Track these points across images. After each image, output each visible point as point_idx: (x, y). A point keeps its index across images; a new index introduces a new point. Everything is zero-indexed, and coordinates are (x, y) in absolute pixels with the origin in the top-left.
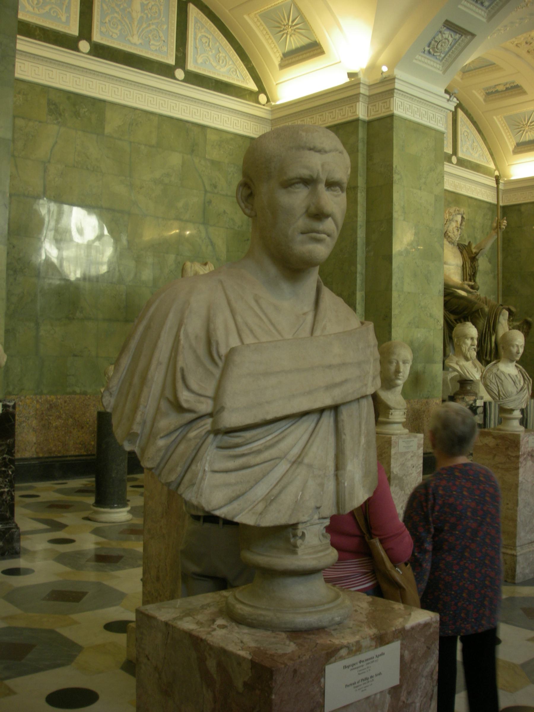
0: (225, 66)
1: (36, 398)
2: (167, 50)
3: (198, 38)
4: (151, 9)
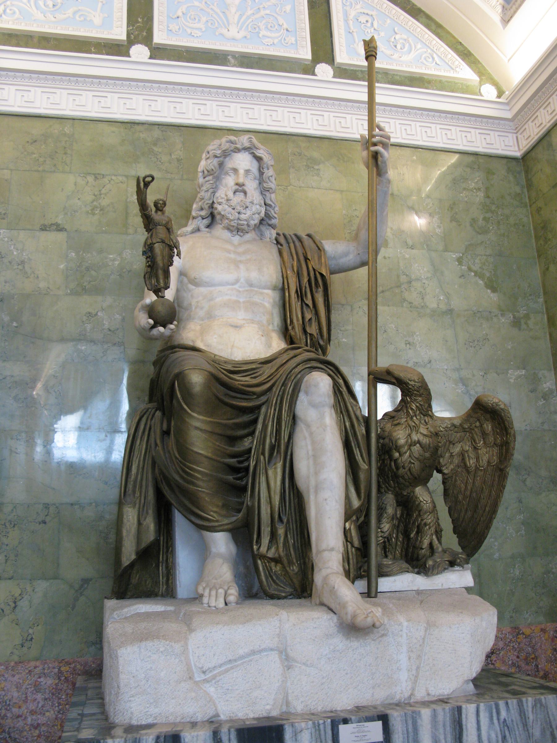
1: (11, 712)
2: (296, 41)
3: (351, 17)
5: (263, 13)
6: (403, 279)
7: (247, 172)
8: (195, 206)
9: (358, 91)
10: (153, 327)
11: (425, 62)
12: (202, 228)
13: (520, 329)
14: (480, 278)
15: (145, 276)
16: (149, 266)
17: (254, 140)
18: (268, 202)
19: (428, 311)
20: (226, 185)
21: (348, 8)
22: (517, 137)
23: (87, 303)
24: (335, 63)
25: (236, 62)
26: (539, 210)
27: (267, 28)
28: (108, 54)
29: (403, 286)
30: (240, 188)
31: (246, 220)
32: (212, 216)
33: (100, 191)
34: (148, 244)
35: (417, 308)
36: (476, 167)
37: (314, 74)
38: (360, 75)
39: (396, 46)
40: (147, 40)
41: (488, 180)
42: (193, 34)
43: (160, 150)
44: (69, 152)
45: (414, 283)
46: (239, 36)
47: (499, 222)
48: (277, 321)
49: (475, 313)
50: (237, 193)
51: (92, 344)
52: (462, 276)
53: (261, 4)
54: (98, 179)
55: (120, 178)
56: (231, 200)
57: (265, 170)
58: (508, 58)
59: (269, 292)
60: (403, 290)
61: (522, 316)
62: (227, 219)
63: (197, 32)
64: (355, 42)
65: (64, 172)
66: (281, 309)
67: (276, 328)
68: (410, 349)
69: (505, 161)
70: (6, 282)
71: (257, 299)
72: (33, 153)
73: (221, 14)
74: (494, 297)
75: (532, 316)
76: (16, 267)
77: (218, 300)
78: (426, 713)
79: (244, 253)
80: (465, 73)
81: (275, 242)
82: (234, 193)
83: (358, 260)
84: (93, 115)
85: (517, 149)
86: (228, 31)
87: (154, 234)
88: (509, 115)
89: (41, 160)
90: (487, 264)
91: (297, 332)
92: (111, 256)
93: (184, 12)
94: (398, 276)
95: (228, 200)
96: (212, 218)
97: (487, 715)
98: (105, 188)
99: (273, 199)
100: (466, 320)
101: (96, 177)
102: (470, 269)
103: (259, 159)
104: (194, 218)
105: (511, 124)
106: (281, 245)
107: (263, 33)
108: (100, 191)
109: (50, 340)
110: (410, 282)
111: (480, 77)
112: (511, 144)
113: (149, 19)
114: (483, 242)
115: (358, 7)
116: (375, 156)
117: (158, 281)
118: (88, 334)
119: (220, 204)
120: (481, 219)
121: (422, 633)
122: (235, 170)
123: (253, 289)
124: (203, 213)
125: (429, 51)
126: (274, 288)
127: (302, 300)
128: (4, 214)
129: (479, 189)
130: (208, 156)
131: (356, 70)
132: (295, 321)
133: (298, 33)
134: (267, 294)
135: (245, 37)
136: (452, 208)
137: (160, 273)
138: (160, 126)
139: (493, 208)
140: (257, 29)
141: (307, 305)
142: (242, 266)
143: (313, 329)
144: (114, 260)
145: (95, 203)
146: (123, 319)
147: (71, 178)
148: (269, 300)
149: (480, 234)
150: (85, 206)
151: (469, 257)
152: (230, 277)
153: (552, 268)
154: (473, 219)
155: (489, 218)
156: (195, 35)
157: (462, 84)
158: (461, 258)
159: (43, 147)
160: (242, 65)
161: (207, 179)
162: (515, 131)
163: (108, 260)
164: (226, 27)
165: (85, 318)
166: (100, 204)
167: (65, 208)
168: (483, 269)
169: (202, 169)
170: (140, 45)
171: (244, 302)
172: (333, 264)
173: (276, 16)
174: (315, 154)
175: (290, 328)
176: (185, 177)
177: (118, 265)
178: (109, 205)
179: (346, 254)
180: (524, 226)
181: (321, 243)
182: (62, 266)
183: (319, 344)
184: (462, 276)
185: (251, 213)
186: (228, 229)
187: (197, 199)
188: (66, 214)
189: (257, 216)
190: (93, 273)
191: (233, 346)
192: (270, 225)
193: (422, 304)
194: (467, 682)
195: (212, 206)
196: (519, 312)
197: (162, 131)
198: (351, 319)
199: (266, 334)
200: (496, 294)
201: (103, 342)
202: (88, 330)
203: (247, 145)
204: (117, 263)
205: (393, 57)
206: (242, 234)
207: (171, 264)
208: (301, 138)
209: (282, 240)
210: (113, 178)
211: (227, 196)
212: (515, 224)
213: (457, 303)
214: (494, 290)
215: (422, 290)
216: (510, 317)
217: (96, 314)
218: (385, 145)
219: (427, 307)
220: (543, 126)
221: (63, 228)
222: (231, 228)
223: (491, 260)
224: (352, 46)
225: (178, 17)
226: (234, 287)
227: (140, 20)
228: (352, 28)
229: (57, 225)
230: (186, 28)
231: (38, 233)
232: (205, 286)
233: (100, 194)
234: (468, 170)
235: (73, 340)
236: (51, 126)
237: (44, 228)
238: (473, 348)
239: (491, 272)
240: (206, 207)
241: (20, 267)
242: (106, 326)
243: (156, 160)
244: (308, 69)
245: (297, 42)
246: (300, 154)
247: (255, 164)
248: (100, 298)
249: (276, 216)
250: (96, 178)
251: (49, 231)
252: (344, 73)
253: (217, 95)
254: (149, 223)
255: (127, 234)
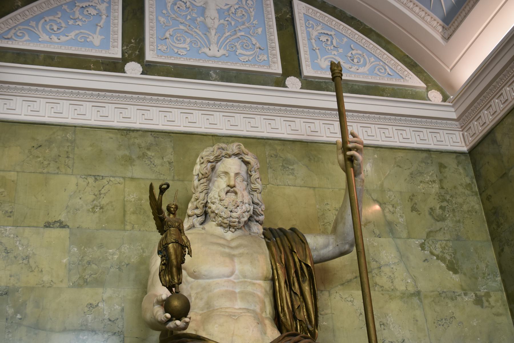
0: (365, 65)
2: (268, 57)
3: (313, 37)
4: (235, 14)
5: (239, 34)
7: (237, 174)
8: (190, 205)
9: (328, 100)
10: (170, 320)
11: (378, 73)
12: (197, 225)
13: (482, 307)
14: (441, 261)
15: (160, 273)
16: (164, 264)
17: (242, 147)
18: (256, 201)
19: (398, 294)
20: (219, 187)
21: (310, 30)
22: (463, 135)
23: (88, 295)
24: (302, 77)
25: (217, 77)
26: (489, 198)
27: (242, 46)
28: (105, 70)
29: (373, 272)
30: (231, 189)
31: (238, 218)
32: (206, 213)
33: (100, 191)
34: (164, 244)
35: (388, 291)
36: (429, 161)
37: (285, 86)
38: (324, 86)
39: (353, 60)
40: (140, 58)
41: (441, 172)
42: (179, 53)
43: (153, 154)
44: (71, 156)
45: (382, 268)
46: (218, 54)
47: (454, 210)
48: (269, 309)
49: (440, 294)
50: (229, 194)
51: (94, 333)
52: (426, 260)
53: (237, 27)
54: (98, 180)
55: (118, 179)
56: (223, 200)
57: (253, 173)
58: (451, 67)
59: (261, 282)
60: (374, 275)
61: (483, 294)
62: (221, 217)
63: (183, 51)
64: (318, 58)
65: (66, 174)
66: (272, 298)
67: (268, 316)
68: (384, 329)
69: (454, 156)
70: (11, 276)
71: (250, 289)
72: (38, 157)
73: (203, 36)
74: (456, 278)
75: (492, 294)
76: (21, 262)
77: (216, 291)
79: (237, 247)
80: (414, 81)
81: (263, 237)
82: (226, 193)
83: (337, 251)
84: (93, 123)
85: (464, 144)
86: (210, 50)
87: (168, 235)
88: (454, 116)
89: (46, 163)
90: (447, 248)
91: (287, 318)
92: (111, 251)
93: (171, 34)
95: (221, 200)
96: (206, 215)
98: (104, 189)
99: (260, 199)
100: (433, 301)
101: (96, 179)
102: (432, 253)
103: (247, 163)
104: (189, 216)
105: (457, 123)
106: (269, 239)
107: (239, 51)
108: (100, 191)
109: (52, 330)
110: (380, 268)
111: (426, 84)
112: (459, 140)
113: (141, 40)
114: (441, 228)
115: (319, 28)
116: (351, 159)
117: (173, 277)
118: (89, 324)
119: (213, 203)
120: (438, 208)
122: (226, 173)
123: (246, 280)
124: (198, 212)
125: (381, 63)
126: (266, 279)
127: (291, 289)
128: (11, 212)
129: (434, 181)
130: (202, 161)
131: (320, 82)
132: (286, 309)
133: (269, 51)
134: (259, 285)
135: (224, 55)
136: (412, 200)
137: (174, 270)
138: (153, 133)
139: (448, 197)
140: (234, 48)
141: (295, 293)
142: (236, 260)
143: (302, 315)
144: (113, 254)
145: (95, 202)
146: (123, 310)
147: (73, 180)
148: (261, 289)
149: (438, 221)
150: (86, 205)
151: (430, 242)
152: (225, 270)
153: (507, 249)
154: (431, 209)
155: (445, 207)
156: (181, 54)
157: (411, 90)
158: (424, 243)
159: (47, 151)
160: (222, 80)
161: (202, 181)
162: (461, 129)
163: (108, 254)
164: (207, 47)
165: (86, 309)
166: (99, 203)
167: (67, 207)
168: (444, 253)
169: (197, 173)
170: (133, 63)
171: (239, 293)
172: (314, 254)
173: (250, 36)
174: (290, 156)
175: (281, 315)
176: (176, 178)
177: (117, 258)
178: (108, 204)
179: (326, 246)
180: (476, 212)
181: (304, 236)
182: (65, 261)
183: (308, 329)
184: (426, 260)
185: (242, 211)
186: (221, 226)
187: (193, 200)
188: (69, 212)
189: (247, 213)
190: (94, 266)
191: (233, 334)
192: (257, 221)
193: (392, 288)
195: (205, 205)
196: (480, 291)
197: (155, 137)
198: (330, 304)
199: (260, 322)
200: (457, 275)
201: (104, 331)
202: (90, 320)
203: (236, 151)
204: (116, 257)
205: (351, 70)
206: (233, 230)
207: (183, 262)
208: (276, 142)
209: (269, 235)
210: (112, 179)
211: (220, 196)
212: (468, 211)
213: (424, 285)
214: (455, 272)
215: (391, 274)
216: (473, 296)
217: (97, 305)
218: (357, 149)
219: (397, 290)
220: (486, 125)
221: (66, 225)
222: (224, 225)
223: (450, 244)
224: (316, 61)
225: (166, 39)
226: (230, 278)
227: (133, 41)
228: (315, 46)
229: (60, 222)
230: (173, 48)
231: (42, 230)
232: (203, 279)
233: (100, 194)
234: (423, 165)
235: (74, 330)
236: (54, 133)
237: (48, 225)
238: (441, 326)
239: (451, 255)
240: (201, 206)
241: (25, 262)
242: (107, 317)
243: (149, 163)
244: (279, 82)
245: (269, 59)
246: (276, 156)
247: (244, 167)
248: (100, 290)
249: (262, 213)
250: (96, 180)
251: (53, 227)
252: (311, 84)
253: (201, 106)
254: (162, 226)
255: (124, 230)
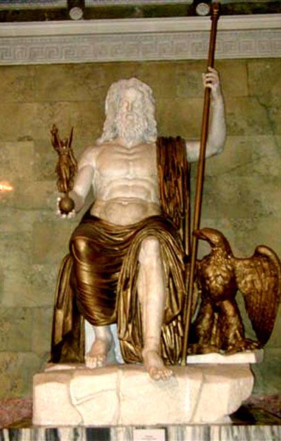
6: (254, 156)
78: (189, 429)
94: (251, 155)
97: (226, 433)
121: (199, 386)
194: (225, 416)
229: (28, 137)
237: (20, 140)
